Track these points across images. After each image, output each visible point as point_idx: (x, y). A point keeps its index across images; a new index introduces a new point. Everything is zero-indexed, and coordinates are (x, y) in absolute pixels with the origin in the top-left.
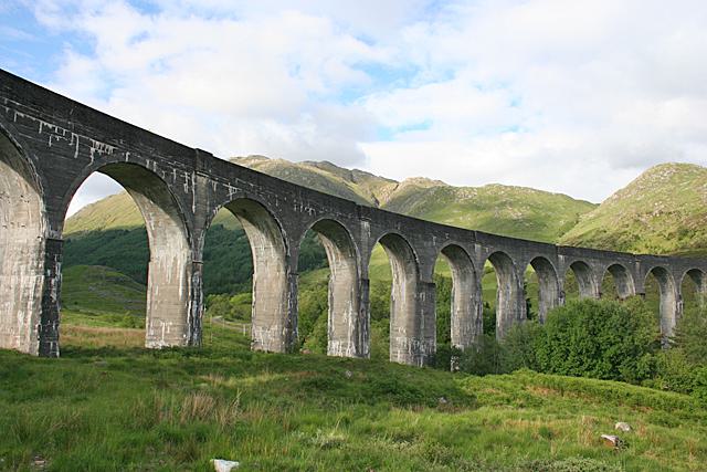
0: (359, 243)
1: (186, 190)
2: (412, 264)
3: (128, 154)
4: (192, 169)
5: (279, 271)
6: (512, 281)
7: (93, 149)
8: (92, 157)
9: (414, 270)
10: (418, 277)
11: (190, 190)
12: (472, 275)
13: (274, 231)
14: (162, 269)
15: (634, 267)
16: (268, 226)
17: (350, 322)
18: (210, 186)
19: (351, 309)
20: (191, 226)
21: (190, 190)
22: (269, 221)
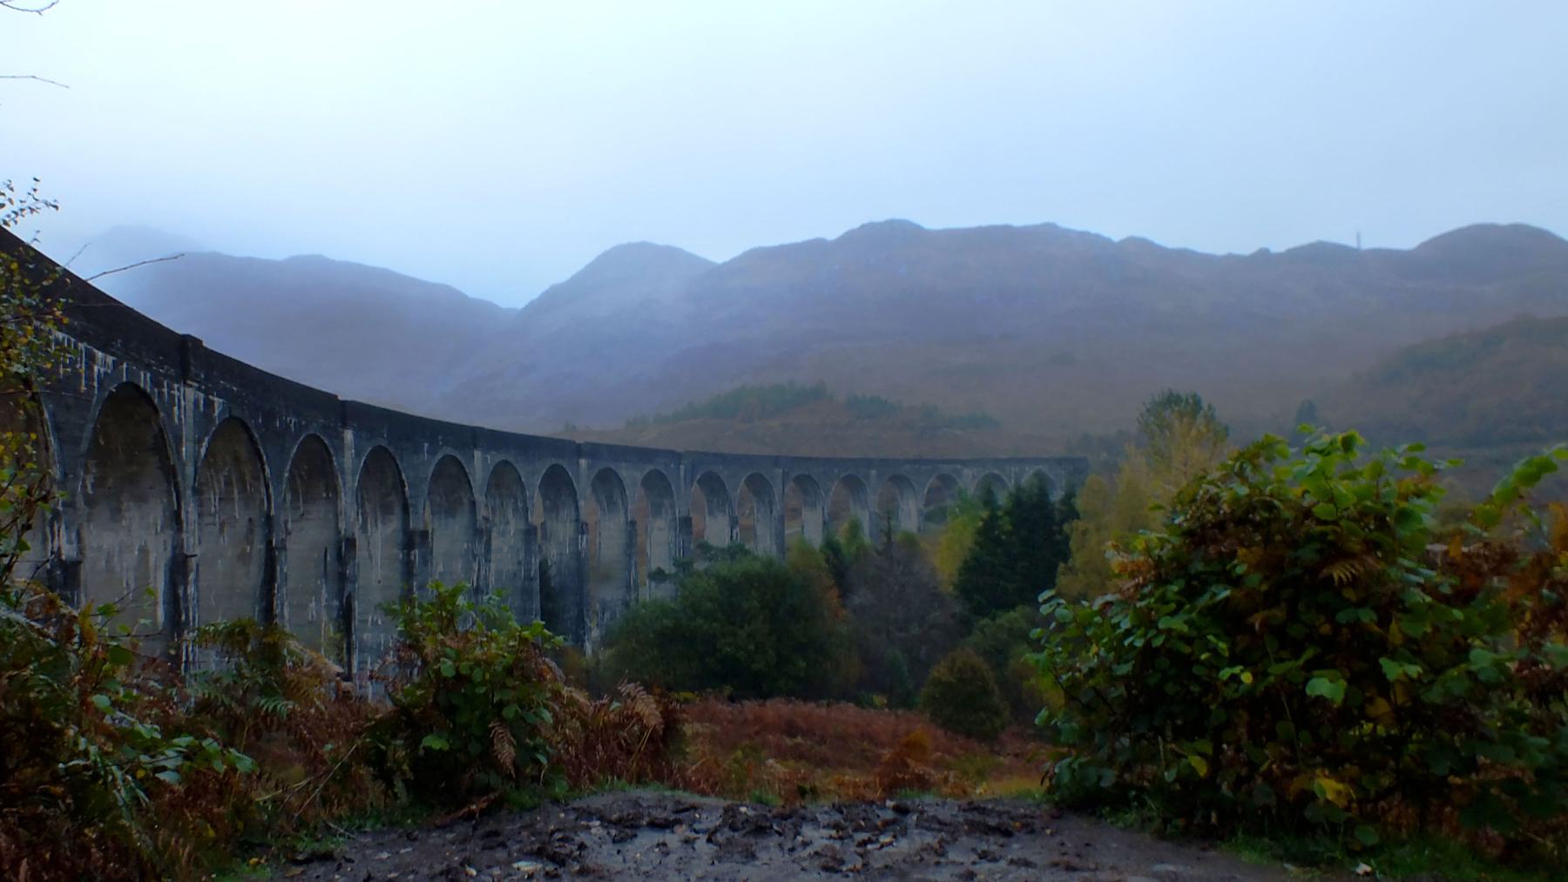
0: (343, 473)
1: (176, 420)
2: (393, 498)
3: (125, 366)
4: (184, 377)
5: (250, 543)
6: (516, 510)
7: (96, 368)
8: (96, 384)
9: (398, 510)
10: (406, 522)
11: (180, 419)
12: (466, 507)
13: (247, 470)
14: (109, 569)
15: (679, 474)
16: (237, 459)
17: (325, 618)
18: (196, 403)
19: (324, 595)
20: (181, 489)
21: (180, 419)
22: (244, 451)
